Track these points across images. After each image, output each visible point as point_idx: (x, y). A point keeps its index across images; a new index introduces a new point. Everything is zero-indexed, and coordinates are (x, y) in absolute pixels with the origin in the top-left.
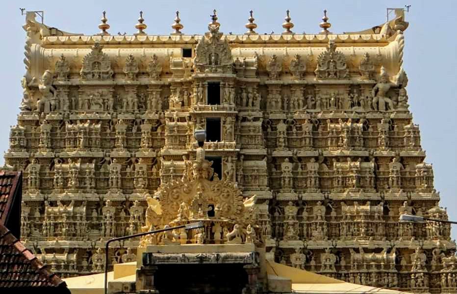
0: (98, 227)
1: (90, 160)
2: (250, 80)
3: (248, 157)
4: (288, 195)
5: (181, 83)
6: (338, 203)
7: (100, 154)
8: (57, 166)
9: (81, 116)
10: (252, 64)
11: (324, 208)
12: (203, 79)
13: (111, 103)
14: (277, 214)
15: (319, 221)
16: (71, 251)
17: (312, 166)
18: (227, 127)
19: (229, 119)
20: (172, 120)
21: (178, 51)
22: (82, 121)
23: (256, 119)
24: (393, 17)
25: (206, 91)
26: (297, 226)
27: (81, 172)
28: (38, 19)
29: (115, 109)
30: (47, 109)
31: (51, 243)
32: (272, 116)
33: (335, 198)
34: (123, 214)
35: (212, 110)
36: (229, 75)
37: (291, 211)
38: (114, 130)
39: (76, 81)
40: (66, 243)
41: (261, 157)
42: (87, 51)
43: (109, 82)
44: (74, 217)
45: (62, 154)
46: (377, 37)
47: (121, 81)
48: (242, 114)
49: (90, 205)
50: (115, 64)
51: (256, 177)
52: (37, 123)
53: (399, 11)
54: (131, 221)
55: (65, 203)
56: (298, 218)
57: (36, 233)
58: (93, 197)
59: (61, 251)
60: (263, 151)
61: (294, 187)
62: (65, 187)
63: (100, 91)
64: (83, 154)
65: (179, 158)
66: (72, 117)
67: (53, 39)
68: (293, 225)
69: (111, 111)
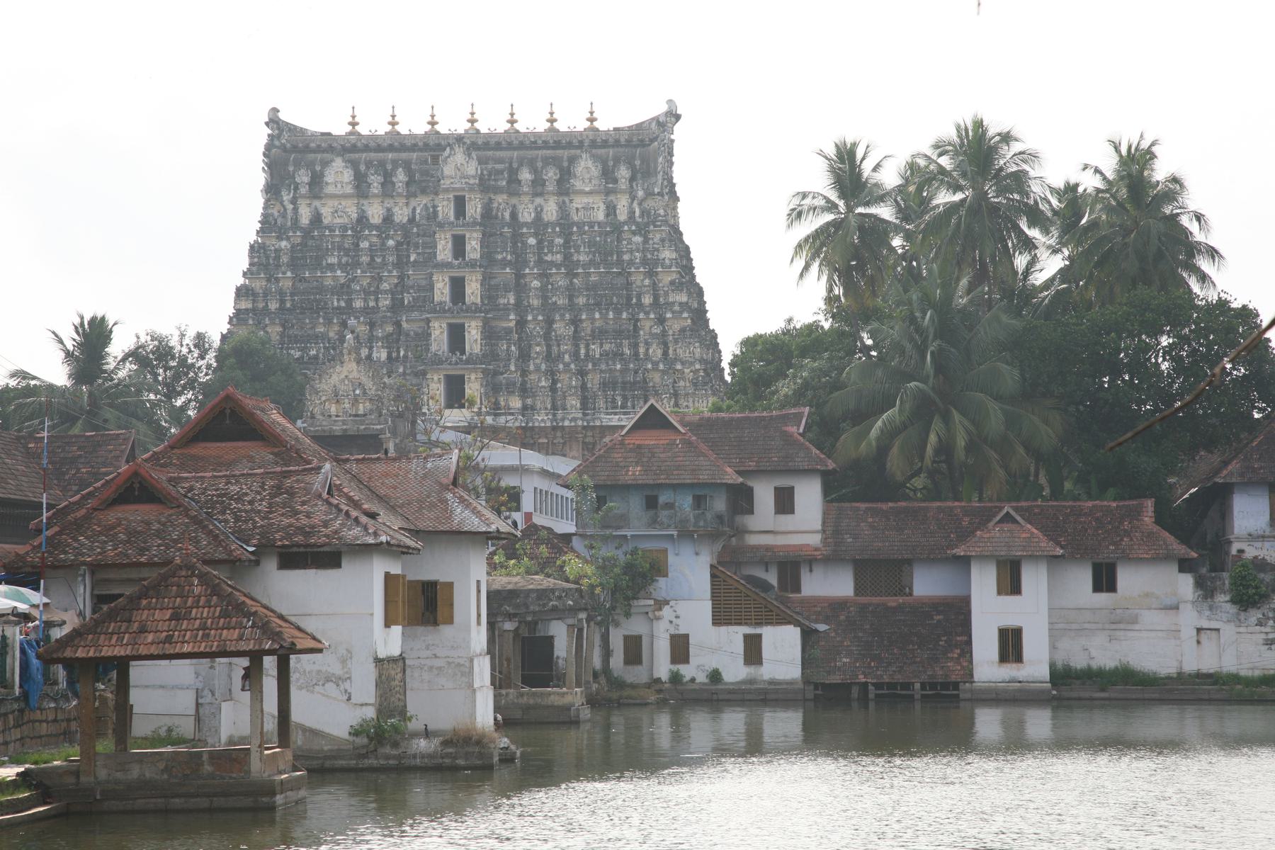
12: (447, 190)
24: (664, 108)
28: (283, 116)
38: (358, 245)
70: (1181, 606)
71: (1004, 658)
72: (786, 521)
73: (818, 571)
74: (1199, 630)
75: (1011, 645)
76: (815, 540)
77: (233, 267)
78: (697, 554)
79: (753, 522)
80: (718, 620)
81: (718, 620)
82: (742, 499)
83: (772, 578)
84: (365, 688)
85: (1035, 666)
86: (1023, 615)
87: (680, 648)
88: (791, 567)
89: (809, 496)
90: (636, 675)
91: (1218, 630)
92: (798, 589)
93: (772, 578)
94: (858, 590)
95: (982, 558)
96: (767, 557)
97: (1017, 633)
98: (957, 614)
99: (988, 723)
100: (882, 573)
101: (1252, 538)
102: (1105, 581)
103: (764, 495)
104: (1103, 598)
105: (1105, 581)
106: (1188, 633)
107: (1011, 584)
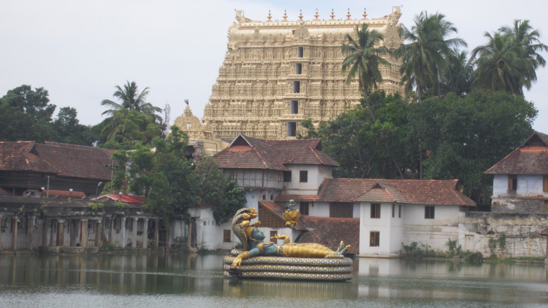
0: (250, 111)
1: (250, 81)
2: (318, 45)
3: (312, 81)
4: (329, 97)
5: (290, 47)
6: (350, 101)
7: (255, 79)
8: (236, 84)
9: (248, 62)
10: (320, 38)
11: (344, 103)
13: (262, 55)
14: (324, 106)
15: (340, 109)
16: (239, 122)
17: (341, 84)
18: (304, 68)
19: (305, 64)
20: (284, 63)
21: (290, 31)
22: (249, 64)
23: (319, 63)
24: (395, 10)
25: (298, 51)
26: (332, 111)
27: (246, 87)
29: (264, 58)
30: (235, 59)
31: (230, 118)
32: (327, 61)
33: (349, 99)
34: (261, 106)
35: (298, 59)
36: (307, 43)
37: (329, 104)
39: (248, 45)
40: (236, 118)
41: (318, 80)
42: (252, 32)
43: (260, 46)
44: (241, 107)
45: (239, 79)
46: (381, 22)
47: (267, 45)
48: (312, 61)
49: (248, 101)
50: (265, 38)
51: (315, 90)
52: (231, 65)
53: (398, 8)
54: (264, 109)
55: (238, 101)
56: (332, 107)
57: (226, 113)
58: (249, 98)
59: (235, 122)
60: (321, 78)
61: (333, 94)
62: (239, 93)
63: (258, 50)
64: (247, 79)
65: (284, 81)
66: (245, 62)
67: (243, 25)
68: (330, 110)
69: (262, 59)
70: (460, 225)
71: (372, 245)
72: (304, 185)
73: (316, 206)
74: (466, 235)
75: (375, 239)
78: (253, 197)
82: (287, 176)
88: (305, 205)
91: (473, 236)
92: (307, 213)
94: (332, 215)
95: (365, 203)
101: (499, 197)
102: (430, 213)
103: (296, 174)
104: (429, 221)
107: (375, 213)
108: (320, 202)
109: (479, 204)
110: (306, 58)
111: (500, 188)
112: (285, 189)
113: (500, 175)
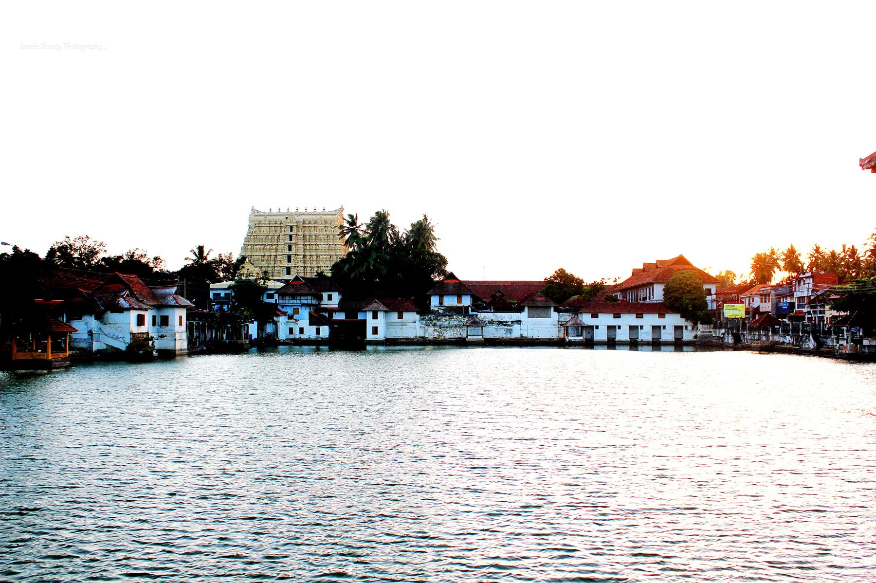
4: (308, 253)
18: (294, 237)
37: (308, 257)
75: (375, 331)
76: (337, 306)
77: (241, 243)
79: (323, 302)
80: (310, 324)
81: (310, 324)
82: (320, 298)
83: (327, 315)
84: (128, 340)
85: (381, 336)
86: (379, 324)
87: (301, 331)
88: (331, 311)
89: (336, 297)
90: (292, 337)
93: (327, 315)
96: (325, 310)
97: (376, 328)
98: (364, 322)
99: (369, 348)
100: (352, 314)
102: (400, 316)
104: (400, 320)
105: (400, 317)
106: (418, 328)
107: (375, 317)
108: (340, 309)
109: (424, 310)
110: (294, 232)
111: (435, 301)
112: (319, 304)
113: (434, 295)
